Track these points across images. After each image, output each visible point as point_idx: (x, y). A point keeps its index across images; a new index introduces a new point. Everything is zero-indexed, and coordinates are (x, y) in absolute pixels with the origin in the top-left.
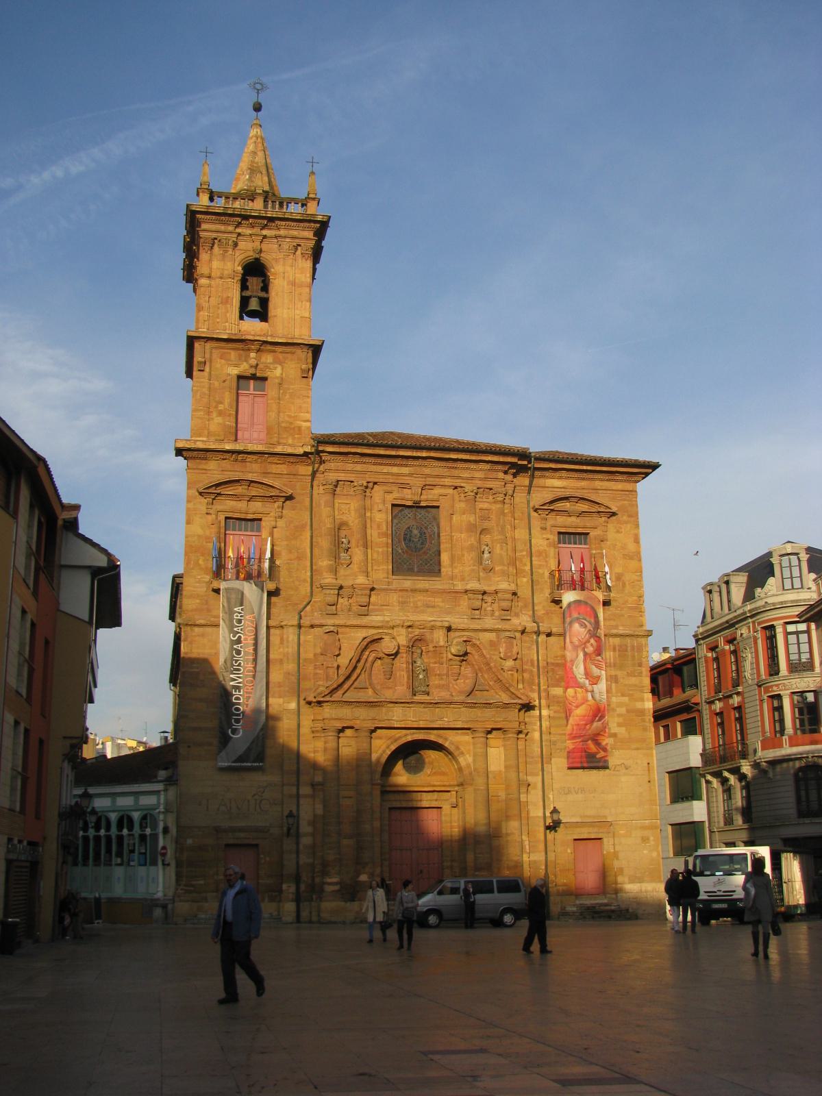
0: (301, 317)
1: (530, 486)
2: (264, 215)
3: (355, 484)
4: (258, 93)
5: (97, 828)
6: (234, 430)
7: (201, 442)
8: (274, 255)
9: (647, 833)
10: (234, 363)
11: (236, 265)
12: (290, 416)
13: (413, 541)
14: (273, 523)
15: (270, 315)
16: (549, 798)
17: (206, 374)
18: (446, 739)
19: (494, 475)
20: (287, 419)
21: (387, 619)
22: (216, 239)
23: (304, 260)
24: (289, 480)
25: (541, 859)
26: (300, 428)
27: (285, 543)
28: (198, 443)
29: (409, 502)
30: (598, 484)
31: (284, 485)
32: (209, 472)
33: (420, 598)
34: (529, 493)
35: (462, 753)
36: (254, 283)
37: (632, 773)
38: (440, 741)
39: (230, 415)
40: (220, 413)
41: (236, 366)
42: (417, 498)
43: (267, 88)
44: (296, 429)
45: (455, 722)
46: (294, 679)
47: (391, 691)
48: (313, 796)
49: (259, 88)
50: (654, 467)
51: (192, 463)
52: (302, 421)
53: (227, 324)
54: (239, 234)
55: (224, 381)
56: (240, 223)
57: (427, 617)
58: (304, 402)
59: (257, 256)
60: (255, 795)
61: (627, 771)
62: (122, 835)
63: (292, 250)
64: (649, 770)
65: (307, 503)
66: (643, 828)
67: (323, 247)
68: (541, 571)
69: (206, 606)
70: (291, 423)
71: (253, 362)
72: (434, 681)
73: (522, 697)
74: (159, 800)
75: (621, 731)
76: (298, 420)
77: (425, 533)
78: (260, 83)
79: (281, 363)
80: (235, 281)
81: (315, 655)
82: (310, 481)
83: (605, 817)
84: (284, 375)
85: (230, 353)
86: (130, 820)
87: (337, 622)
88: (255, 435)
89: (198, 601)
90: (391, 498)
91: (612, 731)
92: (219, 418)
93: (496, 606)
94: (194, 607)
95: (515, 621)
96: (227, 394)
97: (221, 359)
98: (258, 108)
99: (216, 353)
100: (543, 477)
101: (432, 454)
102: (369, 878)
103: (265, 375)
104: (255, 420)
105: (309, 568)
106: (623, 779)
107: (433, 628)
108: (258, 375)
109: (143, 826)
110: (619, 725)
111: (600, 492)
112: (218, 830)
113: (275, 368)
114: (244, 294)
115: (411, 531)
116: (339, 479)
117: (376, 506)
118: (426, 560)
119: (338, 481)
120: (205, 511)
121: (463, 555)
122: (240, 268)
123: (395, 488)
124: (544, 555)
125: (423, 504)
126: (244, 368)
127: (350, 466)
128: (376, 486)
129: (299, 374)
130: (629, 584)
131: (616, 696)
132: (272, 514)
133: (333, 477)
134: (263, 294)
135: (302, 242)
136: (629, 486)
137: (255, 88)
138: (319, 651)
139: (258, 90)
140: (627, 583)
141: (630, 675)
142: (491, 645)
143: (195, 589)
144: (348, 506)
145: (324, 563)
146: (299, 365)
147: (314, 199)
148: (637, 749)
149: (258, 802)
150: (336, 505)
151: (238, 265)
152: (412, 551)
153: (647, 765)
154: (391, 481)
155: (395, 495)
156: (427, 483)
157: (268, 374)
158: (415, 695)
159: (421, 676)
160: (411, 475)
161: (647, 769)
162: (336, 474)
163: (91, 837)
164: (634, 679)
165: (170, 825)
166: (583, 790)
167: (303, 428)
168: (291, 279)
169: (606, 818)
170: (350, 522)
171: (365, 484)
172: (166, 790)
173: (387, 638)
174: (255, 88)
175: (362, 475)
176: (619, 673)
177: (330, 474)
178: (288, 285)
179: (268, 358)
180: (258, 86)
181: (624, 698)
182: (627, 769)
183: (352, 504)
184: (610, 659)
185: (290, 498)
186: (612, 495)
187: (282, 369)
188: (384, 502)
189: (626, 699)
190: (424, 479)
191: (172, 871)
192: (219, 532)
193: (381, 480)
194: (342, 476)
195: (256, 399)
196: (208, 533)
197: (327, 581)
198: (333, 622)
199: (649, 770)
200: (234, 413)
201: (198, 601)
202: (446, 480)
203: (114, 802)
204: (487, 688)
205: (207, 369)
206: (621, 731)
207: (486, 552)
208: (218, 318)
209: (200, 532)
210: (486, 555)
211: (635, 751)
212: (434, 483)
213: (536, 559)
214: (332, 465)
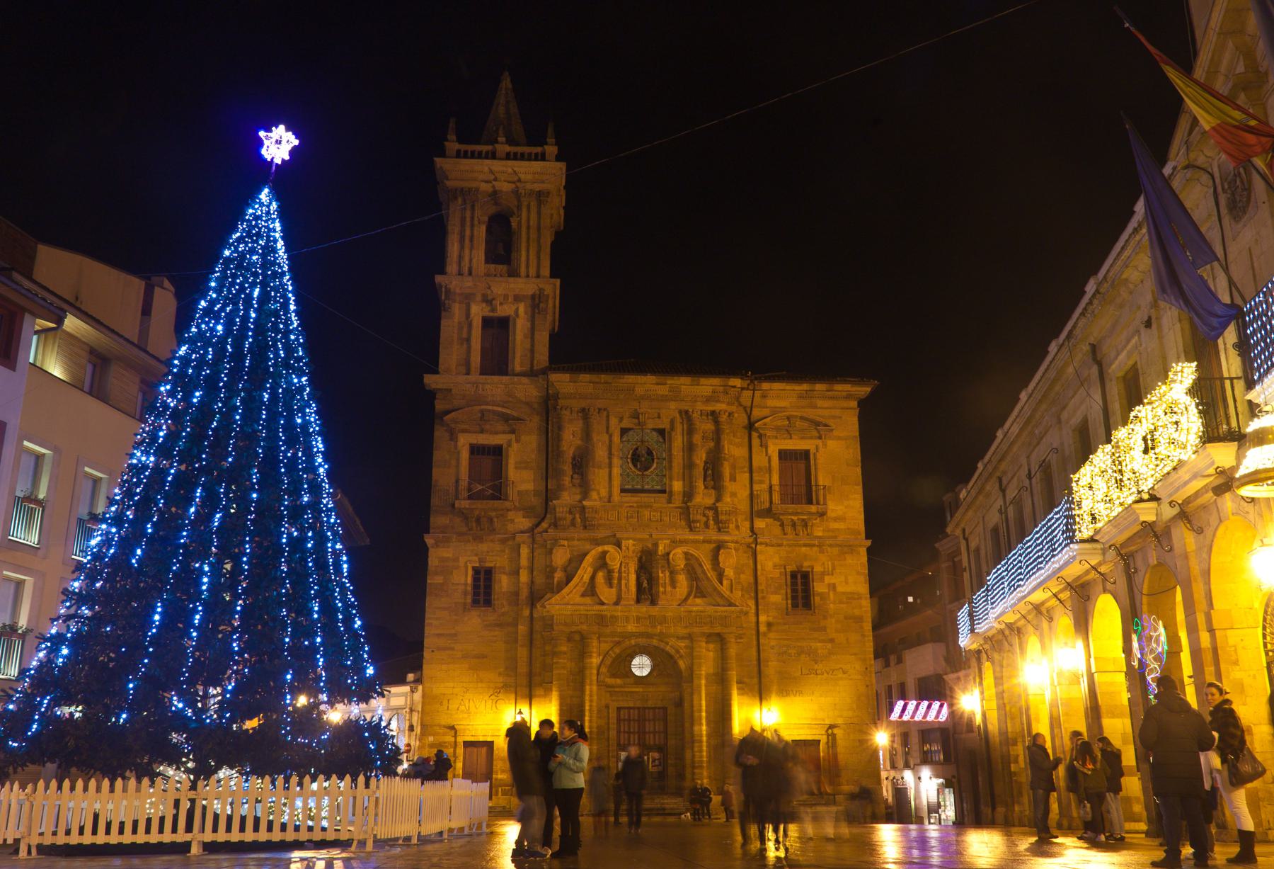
18: (667, 644)
30: (820, 403)
38: (662, 645)
61: (844, 676)
74: (406, 701)
165: (415, 724)
181: (842, 605)
182: (844, 673)
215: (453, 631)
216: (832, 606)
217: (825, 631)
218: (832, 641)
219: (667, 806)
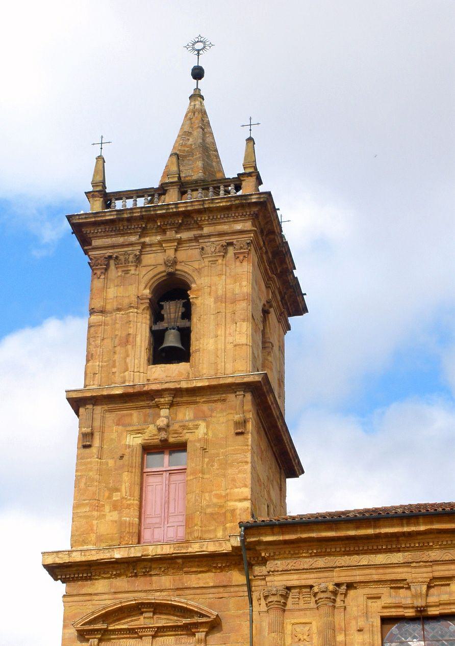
0: (235, 346)
2: (175, 210)
3: (316, 589)
4: (198, 54)
6: (135, 530)
7: (79, 553)
8: (196, 265)
10: (135, 428)
11: (142, 286)
12: (218, 496)
15: (193, 349)
17: (94, 450)
20: (215, 500)
22: (110, 257)
23: (238, 263)
24: (217, 596)
26: (233, 511)
28: (74, 554)
29: (411, 610)
31: (210, 606)
32: (96, 598)
36: (172, 310)
39: (128, 507)
40: (115, 507)
41: (139, 432)
42: (420, 602)
43: (211, 45)
44: (229, 515)
51: (78, 587)
52: (236, 501)
53: (126, 373)
54: (144, 245)
55: (122, 457)
56: (144, 229)
58: (239, 472)
59: (171, 270)
63: (219, 252)
65: (246, 631)
70: (221, 507)
71: (162, 422)
76: (232, 500)
78: (201, 42)
79: (204, 418)
82: (246, 594)
84: (210, 434)
85: (131, 415)
88: (171, 534)
92: (111, 514)
97: (118, 425)
99: (111, 417)
103: (183, 439)
104: (172, 510)
108: (171, 440)
113: (197, 427)
114: (155, 328)
116: (289, 584)
117: (353, 623)
119: (289, 588)
122: (147, 292)
123: (384, 590)
125: (433, 611)
126: (150, 434)
127: (306, 563)
128: (352, 593)
129: (232, 431)
133: (278, 582)
134: (182, 323)
135: (234, 239)
139: (198, 51)
144: (307, 628)
146: (231, 417)
150: (288, 628)
151: (145, 288)
154: (376, 577)
155: (386, 600)
156: (437, 574)
157: (187, 436)
160: (407, 564)
162: (285, 577)
167: (238, 512)
168: (220, 292)
171: (331, 587)
174: (194, 49)
175: (326, 574)
177: (276, 578)
178: (215, 302)
179: (185, 414)
180: (199, 46)
183: (314, 623)
185: (214, 626)
187: (207, 427)
188: (366, 614)
190: (429, 569)
193: (358, 579)
194: (294, 580)
195: (174, 477)
200: (137, 502)
205: (96, 443)
208: (114, 366)
212: (447, 574)
214: (279, 564)
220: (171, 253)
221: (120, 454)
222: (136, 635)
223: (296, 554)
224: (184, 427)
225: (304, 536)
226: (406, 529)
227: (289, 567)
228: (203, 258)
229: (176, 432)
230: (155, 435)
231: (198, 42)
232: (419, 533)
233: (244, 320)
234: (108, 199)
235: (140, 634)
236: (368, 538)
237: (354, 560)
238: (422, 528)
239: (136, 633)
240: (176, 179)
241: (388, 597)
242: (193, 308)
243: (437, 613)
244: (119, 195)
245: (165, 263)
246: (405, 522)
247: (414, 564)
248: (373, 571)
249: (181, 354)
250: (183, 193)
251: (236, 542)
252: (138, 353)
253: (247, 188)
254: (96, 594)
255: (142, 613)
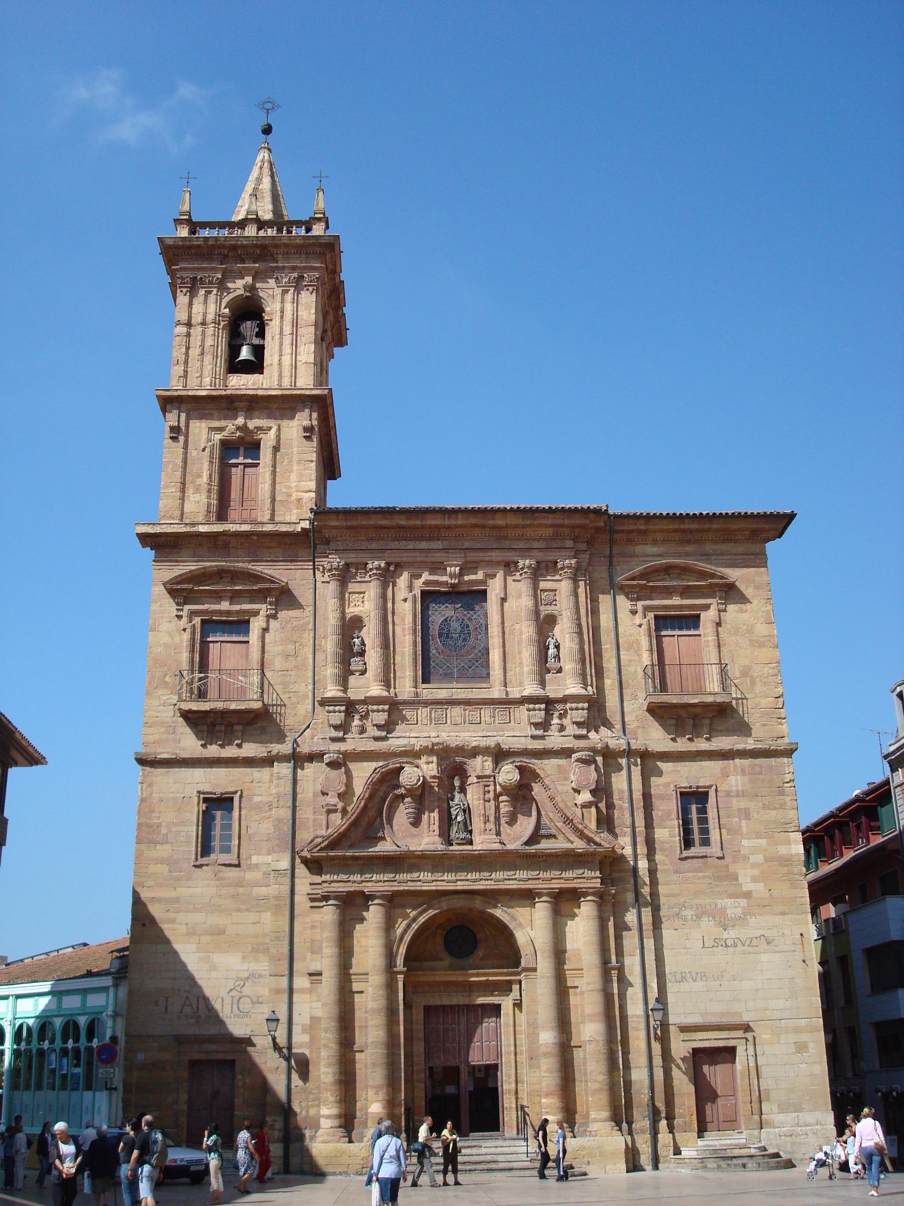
1: (611, 557)
5: (65, 1041)
9: (804, 1037)
11: (223, 305)
13: (452, 637)
14: (264, 625)
16: (652, 988)
19: (560, 545)
20: (284, 490)
21: (413, 741)
25: (642, 1078)
27: (280, 648)
30: (709, 548)
33: (456, 712)
34: (611, 564)
35: (520, 925)
37: (777, 949)
40: (197, 490)
41: (221, 429)
43: (279, 106)
45: (507, 882)
46: (287, 828)
47: (415, 840)
48: (310, 991)
49: (269, 106)
50: (791, 517)
52: (302, 492)
55: (204, 450)
57: (470, 737)
59: (248, 294)
60: (231, 990)
62: (92, 1047)
63: (292, 283)
64: (802, 944)
66: (797, 1030)
67: (343, 282)
68: (632, 669)
69: (171, 736)
71: (240, 421)
72: (477, 824)
73: (603, 843)
75: (759, 889)
77: (468, 626)
80: (221, 327)
81: (315, 795)
83: (740, 1014)
86: (76, 1025)
87: (343, 747)
89: (162, 730)
90: (419, 584)
91: (744, 889)
92: (195, 495)
93: (567, 721)
94: (157, 737)
95: (592, 735)
96: (206, 465)
98: (267, 130)
100: (630, 541)
101: (472, 521)
102: (384, 1108)
105: (311, 681)
106: (765, 958)
107: (475, 752)
109: (90, 1038)
110: (754, 880)
111: (713, 557)
112: (181, 1040)
113: (270, 429)
114: (233, 343)
115: (449, 625)
118: (470, 661)
120: (175, 613)
121: (520, 652)
122: (227, 310)
124: (635, 646)
127: (364, 545)
130: (761, 681)
131: (749, 839)
132: (261, 613)
134: (256, 341)
136: (755, 548)
137: (263, 107)
138: (319, 788)
139: (268, 110)
140: (758, 679)
141: (765, 807)
142: (560, 773)
143: (158, 714)
144: (362, 595)
145: (330, 671)
147: (319, 219)
148: (783, 914)
149: (235, 1000)
151: (225, 308)
152: (450, 650)
153: (799, 936)
154: (419, 559)
156: (468, 559)
158: (452, 845)
159: (459, 819)
161: (800, 942)
163: (34, 1051)
164: (773, 812)
166: (703, 976)
167: (304, 501)
169: (741, 1017)
170: (364, 616)
172: (116, 985)
173: (408, 769)
176: (751, 805)
180: (268, 106)
184: (737, 786)
186: (729, 561)
189: (763, 842)
191: (118, 1097)
192: (193, 639)
193: (405, 559)
195: (247, 470)
196: (177, 640)
197: (329, 694)
198: (338, 749)
199: (802, 944)
201: (162, 730)
202: (493, 554)
203: (84, 1001)
204: (553, 831)
206: (759, 889)
207: (552, 646)
209: (166, 639)
210: (552, 651)
211: (781, 917)
213: (625, 652)
215: (172, 894)
216: (745, 842)
217: (737, 879)
218: (748, 895)
219: (500, 1158)
220: (249, 280)
221: (202, 447)
222: (216, 595)
223: (354, 537)
224: (259, 428)
225: (363, 523)
226: (447, 522)
227: (349, 548)
228: (278, 287)
229: (252, 432)
230: (233, 433)
231: (268, 102)
232: (456, 526)
233: (310, 342)
234: (194, 227)
235: (220, 595)
236: (415, 528)
237: (403, 545)
238: (460, 522)
239: (217, 593)
240: (254, 217)
241: (426, 576)
242: (267, 328)
243: (466, 589)
244: (204, 225)
245: (244, 287)
246: (446, 516)
247: (451, 551)
248: (418, 554)
249: (256, 366)
250: (259, 229)
251: (306, 525)
252: (218, 365)
253: (318, 230)
254: (182, 561)
255: (222, 578)
